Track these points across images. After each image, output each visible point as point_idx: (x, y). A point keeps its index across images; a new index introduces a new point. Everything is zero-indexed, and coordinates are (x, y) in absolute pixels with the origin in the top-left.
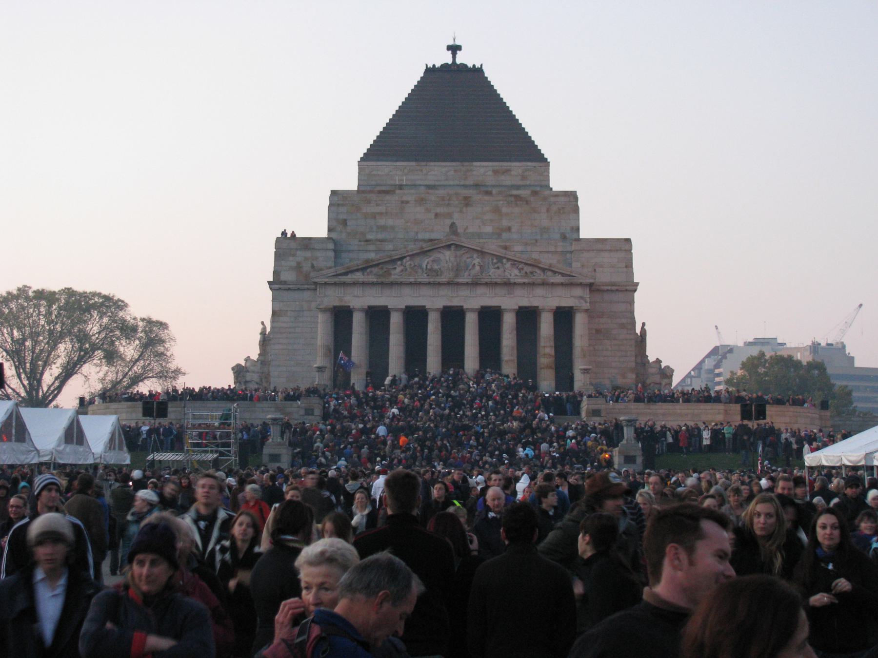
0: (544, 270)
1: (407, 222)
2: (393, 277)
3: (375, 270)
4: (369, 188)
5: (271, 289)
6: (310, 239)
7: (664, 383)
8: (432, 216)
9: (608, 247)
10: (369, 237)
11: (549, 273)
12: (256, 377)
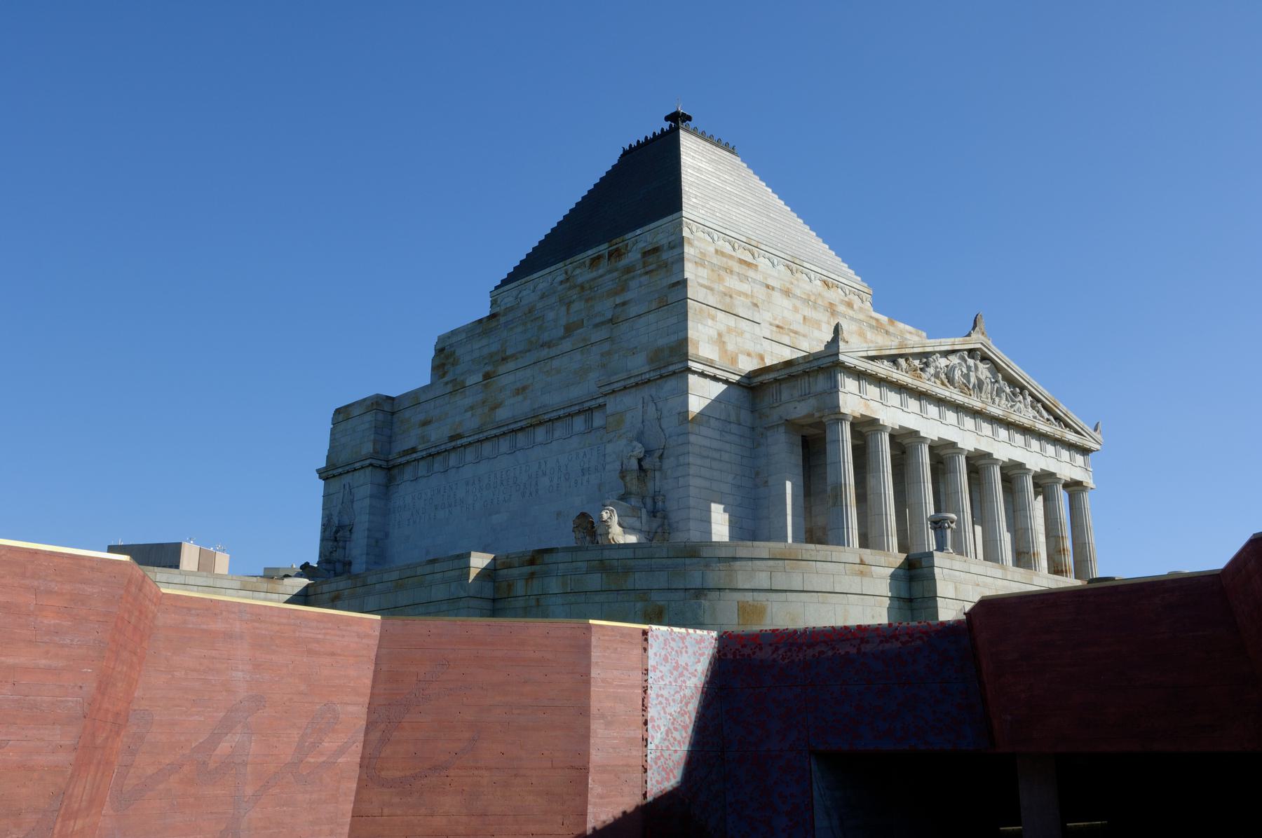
0: (1057, 418)
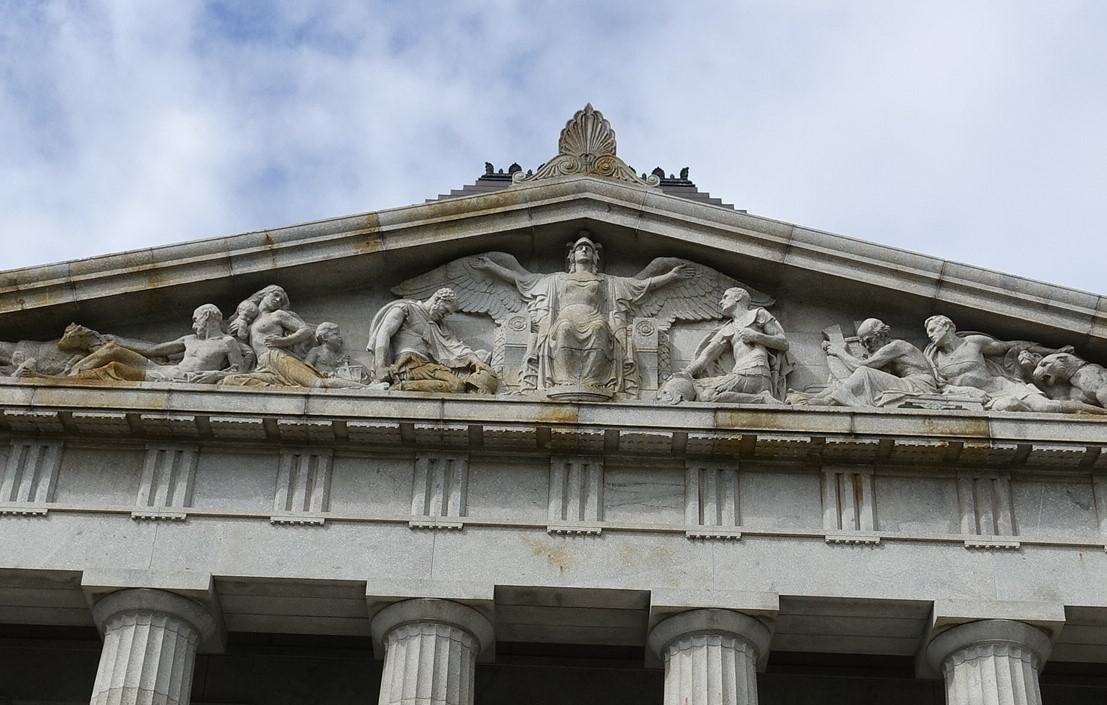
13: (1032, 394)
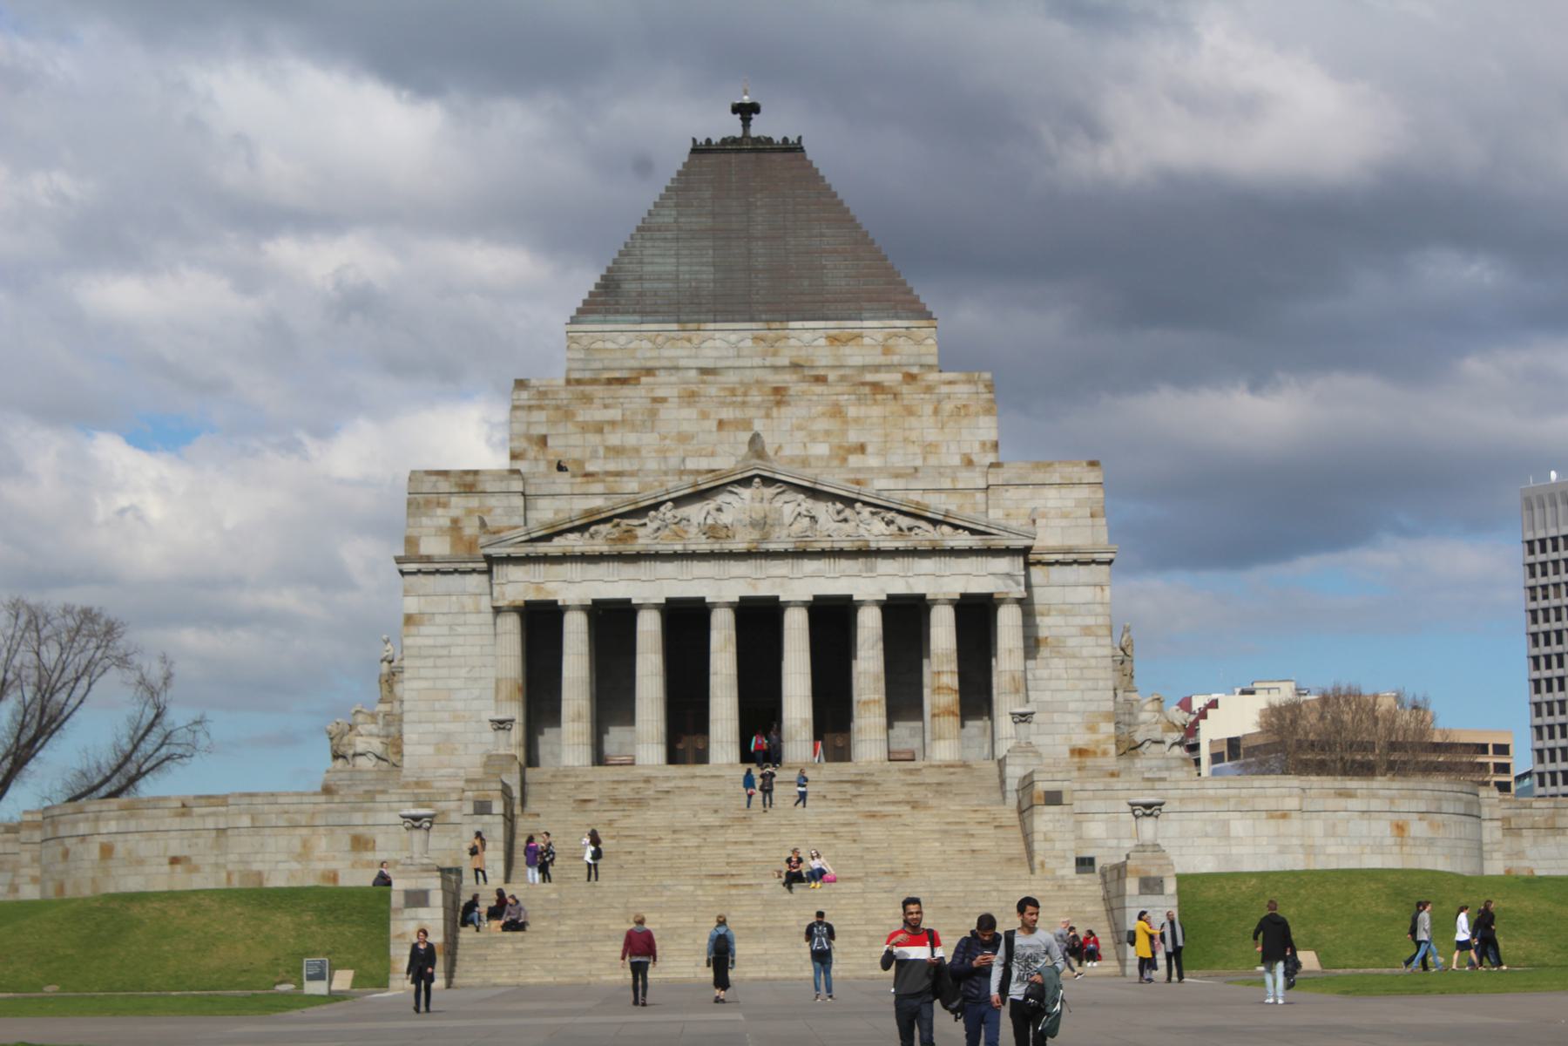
1: (665, 438)
2: (640, 541)
3: (604, 529)
4: (588, 375)
5: (403, 573)
6: (476, 472)
7: (1169, 741)
8: (713, 425)
9: (1056, 478)
10: (590, 468)
11: (946, 529)
12: (376, 745)
13: (883, 525)
